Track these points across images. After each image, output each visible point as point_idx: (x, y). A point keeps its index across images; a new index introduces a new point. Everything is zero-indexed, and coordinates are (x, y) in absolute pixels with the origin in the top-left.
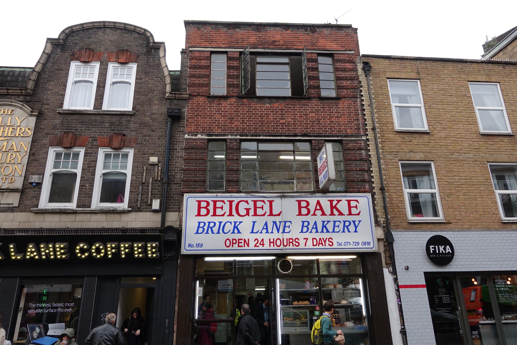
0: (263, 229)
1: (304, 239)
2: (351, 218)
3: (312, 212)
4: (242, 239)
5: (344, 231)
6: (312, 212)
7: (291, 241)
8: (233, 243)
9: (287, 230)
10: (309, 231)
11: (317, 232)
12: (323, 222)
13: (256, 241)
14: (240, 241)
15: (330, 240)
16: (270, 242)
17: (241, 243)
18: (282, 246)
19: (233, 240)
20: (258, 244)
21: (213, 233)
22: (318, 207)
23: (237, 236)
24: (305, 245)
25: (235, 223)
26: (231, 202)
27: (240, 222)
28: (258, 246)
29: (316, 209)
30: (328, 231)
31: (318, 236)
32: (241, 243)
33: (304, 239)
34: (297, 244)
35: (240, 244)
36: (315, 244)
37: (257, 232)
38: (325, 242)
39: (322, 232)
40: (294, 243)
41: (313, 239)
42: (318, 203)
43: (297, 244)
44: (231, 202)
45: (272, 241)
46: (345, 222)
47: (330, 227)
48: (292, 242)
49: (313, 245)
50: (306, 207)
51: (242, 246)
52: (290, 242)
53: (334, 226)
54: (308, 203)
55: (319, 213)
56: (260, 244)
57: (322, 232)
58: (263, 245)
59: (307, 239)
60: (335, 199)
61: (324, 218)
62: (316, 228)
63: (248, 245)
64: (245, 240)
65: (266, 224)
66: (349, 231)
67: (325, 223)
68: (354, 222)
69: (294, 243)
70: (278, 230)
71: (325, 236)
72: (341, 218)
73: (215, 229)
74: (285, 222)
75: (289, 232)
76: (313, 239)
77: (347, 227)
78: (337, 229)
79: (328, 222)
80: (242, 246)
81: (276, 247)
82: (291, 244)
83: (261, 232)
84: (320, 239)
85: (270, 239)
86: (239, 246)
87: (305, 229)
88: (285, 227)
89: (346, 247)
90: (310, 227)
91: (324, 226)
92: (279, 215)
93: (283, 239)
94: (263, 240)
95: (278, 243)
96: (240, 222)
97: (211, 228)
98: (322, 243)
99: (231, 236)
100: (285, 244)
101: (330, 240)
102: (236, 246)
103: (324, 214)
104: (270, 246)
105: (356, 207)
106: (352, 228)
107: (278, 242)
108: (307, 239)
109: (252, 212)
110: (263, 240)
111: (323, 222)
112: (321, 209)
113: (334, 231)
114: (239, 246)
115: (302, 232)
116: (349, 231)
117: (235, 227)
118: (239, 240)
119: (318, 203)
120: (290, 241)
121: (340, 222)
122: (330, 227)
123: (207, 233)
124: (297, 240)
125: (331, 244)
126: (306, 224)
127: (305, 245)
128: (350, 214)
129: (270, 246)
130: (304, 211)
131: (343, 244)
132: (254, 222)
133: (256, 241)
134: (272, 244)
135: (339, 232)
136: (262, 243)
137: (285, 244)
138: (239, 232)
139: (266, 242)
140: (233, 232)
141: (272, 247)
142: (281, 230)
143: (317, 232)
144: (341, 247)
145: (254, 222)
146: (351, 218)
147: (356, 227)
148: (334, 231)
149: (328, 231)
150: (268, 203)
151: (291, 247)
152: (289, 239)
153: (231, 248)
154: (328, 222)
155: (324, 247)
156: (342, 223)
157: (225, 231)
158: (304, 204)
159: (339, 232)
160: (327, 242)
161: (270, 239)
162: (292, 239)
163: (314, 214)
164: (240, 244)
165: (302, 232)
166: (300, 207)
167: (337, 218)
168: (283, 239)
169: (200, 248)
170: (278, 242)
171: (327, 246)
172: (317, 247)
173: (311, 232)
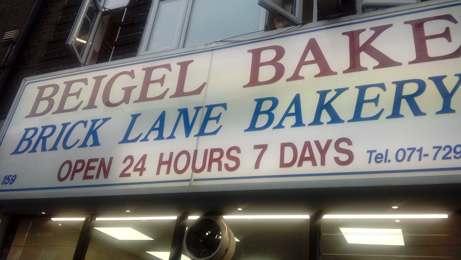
0: (153, 129)
1: (256, 147)
2: (424, 71)
3: (289, 72)
4: (96, 160)
5: (396, 114)
6: (289, 72)
7: (216, 155)
8: (76, 171)
9: (211, 126)
10: (276, 122)
11: (299, 123)
12: (323, 94)
13: (129, 161)
14: (92, 164)
15: (343, 145)
16: (161, 163)
17: (93, 168)
18: (188, 174)
19: (78, 162)
20: (130, 171)
21: (44, 149)
22: (310, 57)
23: (87, 154)
24: (257, 166)
25: (94, 122)
26: (99, 80)
27: (105, 120)
28: (129, 175)
29: (302, 63)
30: (335, 119)
31: (300, 136)
32: (93, 168)
33: (256, 147)
34: (232, 164)
35: (90, 173)
36: (288, 158)
37: (135, 140)
38: (323, 152)
39: (317, 121)
40: (225, 160)
41: (283, 146)
42: (312, 45)
43: (232, 164)
44: (99, 80)
45: (166, 159)
46: (400, 85)
47: (345, 105)
48: (218, 160)
49: (283, 165)
50: (274, 62)
51: (91, 177)
52: (212, 160)
53: (361, 102)
54: (280, 52)
55: (310, 71)
56: (135, 170)
57: (317, 121)
58: (142, 170)
59: (264, 147)
60: (367, 26)
61: (328, 83)
62: (298, 114)
63: (106, 174)
64: (103, 160)
65: (162, 118)
66: (417, 111)
67: (328, 97)
68: (438, 81)
69: (225, 160)
70: (188, 129)
71: (326, 132)
72: (389, 76)
73: (50, 142)
74: (210, 108)
75: (215, 133)
76: (283, 146)
77: (410, 99)
78: (368, 110)
79: (340, 91)
80: (91, 177)
81: (173, 175)
82: (215, 165)
83: (146, 139)
84: (307, 145)
85: (162, 155)
86: (86, 177)
87: (262, 120)
88: (207, 118)
89: (405, 165)
90: (279, 113)
91: (324, 105)
92: (198, 91)
93: (196, 152)
94: (144, 158)
95: (181, 164)
96: (105, 120)
97: (44, 139)
98: (312, 158)
99: (75, 154)
100: (199, 165)
101: (343, 145)
102: (79, 176)
103: (325, 71)
104: (158, 173)
105: (446, 34)
106: (431, 99)
107: (183, 159)
108: (264, 147)
109: (136, 94)
110: (144, 158)
111: (323, 94)
112: (320, 59)
113: (357, 117)
114: (86, 177)
115: (252, 128)
116: (417, 111)
117: (93, 132)
118: (91, 161)
119: (312, 45)
120: (212, 157)
121: (382, 86)
122: (345, 105)
123: (34, 150)
124: (234, 153)
125: (344, 157)
126: (266, 106)
127: (257, 166)
128: (422, 56)
129: (158, 173)
130: (267, 73)
131: (391, 156)
132: (135, 117)
133: (129, 161)
134: (164, 168)
135: (376, 117)
136: (139, 166)
137: (199, 165)
138: (96, 143)
139: (151, 165)
140: (84, 145)
141: (163, 176)
142: (196, 130)
143: (299, 123)
144: (383, 166)
145: (135, 117)
146: (424, 71)
147: (447, 96)
148: (357, 117)
149: (335, 119)
150: (176, 69)
151: (215, 172)
152: (213, 151)
153: (68, 182)
154: (340, 91)
155: (319, 169)
156: (392, 90)
157: (69, 144)
158: (268, 55)
159: (376, 117)
160: (332, 153)
161: (162, 155)
162: (220, 150)
163: (296, 77)
164: (90, 173)
165: (252, 128)
166: (256, 65)
167: (370, 73)
168: (196, 152)
169: (8, 187)
170: (183, 159)
171: (331, 166)
172: (294, 170)
173: (280, 126)
